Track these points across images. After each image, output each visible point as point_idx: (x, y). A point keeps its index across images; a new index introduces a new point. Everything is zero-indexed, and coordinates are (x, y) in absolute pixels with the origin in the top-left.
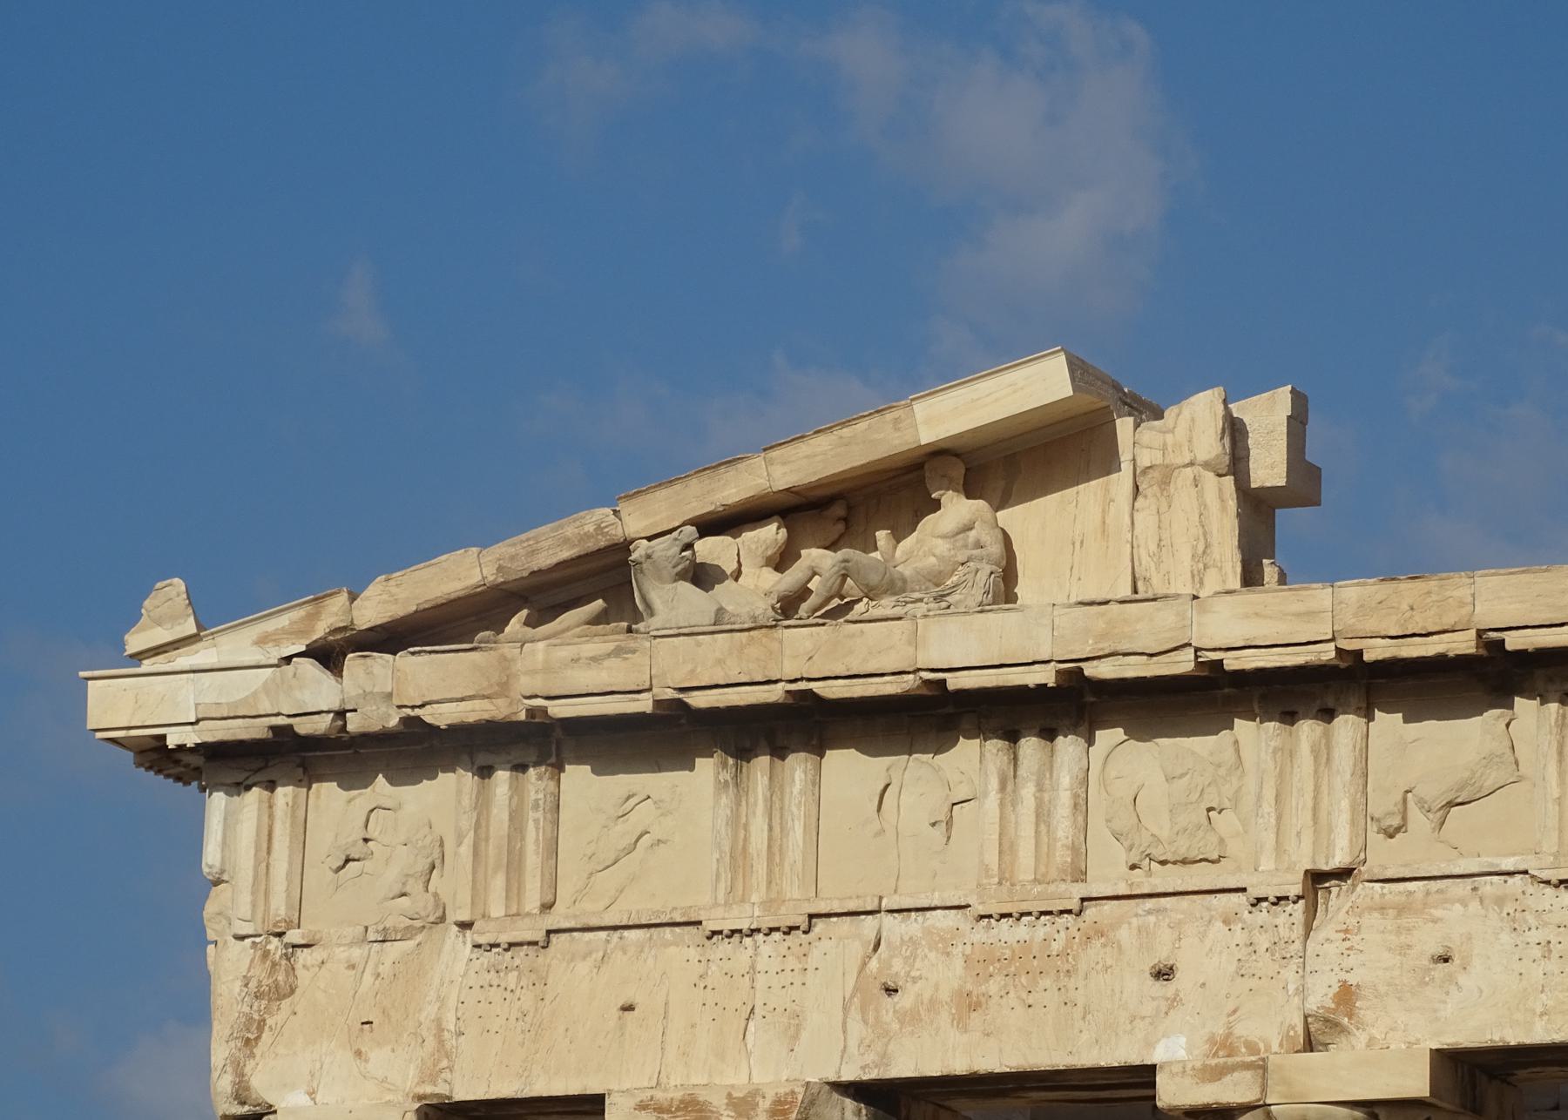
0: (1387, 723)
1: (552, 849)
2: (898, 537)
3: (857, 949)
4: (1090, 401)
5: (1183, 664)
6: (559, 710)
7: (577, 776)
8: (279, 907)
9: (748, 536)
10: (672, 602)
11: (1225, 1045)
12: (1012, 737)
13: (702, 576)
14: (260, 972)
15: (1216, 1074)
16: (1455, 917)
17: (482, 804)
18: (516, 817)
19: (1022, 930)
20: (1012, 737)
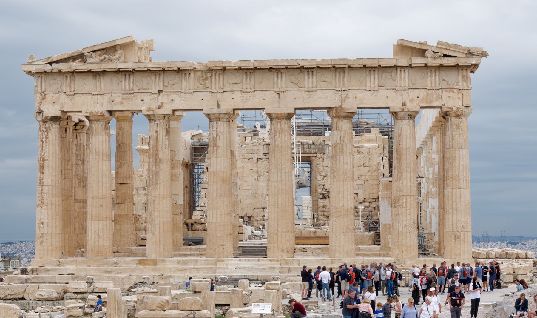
5: (146, 69)
10: (90, 60)
11: (149, 108)
14: (41, 96)
15: (149, 111)
16: (173, 96)
19: (127, 96)
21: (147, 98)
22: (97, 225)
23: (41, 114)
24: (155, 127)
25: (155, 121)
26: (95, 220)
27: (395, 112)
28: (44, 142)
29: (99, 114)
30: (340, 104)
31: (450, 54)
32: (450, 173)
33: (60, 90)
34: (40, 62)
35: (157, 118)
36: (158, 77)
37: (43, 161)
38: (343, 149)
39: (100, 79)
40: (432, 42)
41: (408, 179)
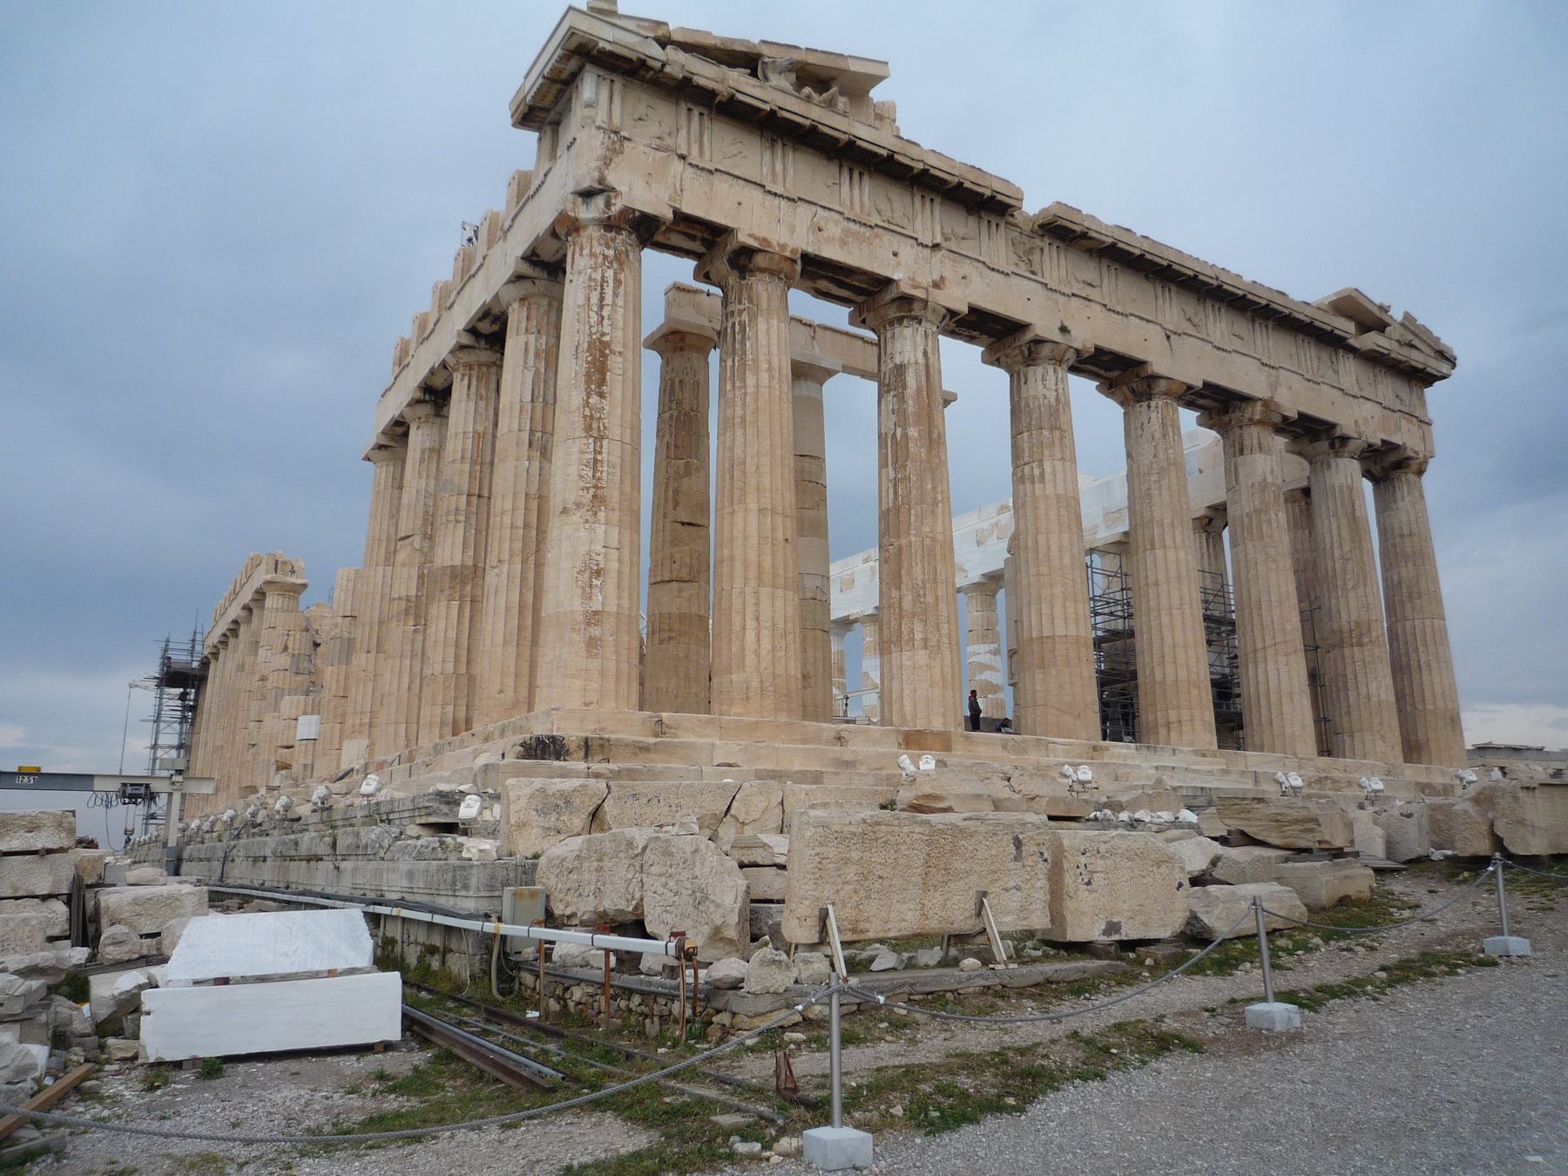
5: (921, 166)
15: (916, 287)
16: (967, 268)
21: (908, 252)
23: (599, 201)
24: (919, 338)
25: (920, 323)
27: (1345, 439)
28: (609, 291)
29: (788, 254)
33: (669, 141)
34: (631, 25)
35: (929, 315)
36: (928, 204)
37: (603, 355)
40: (1397, 314)
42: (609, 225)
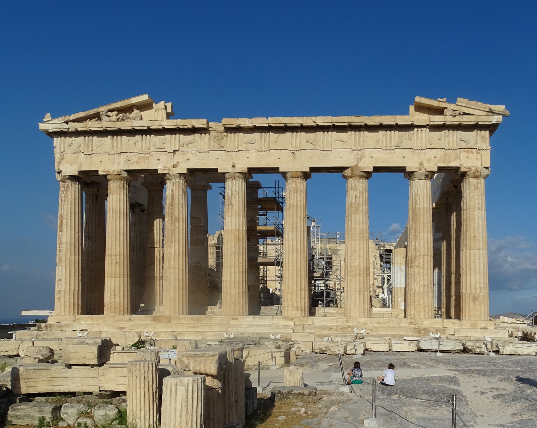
0: (182, 136)
1: (92, 145)
2: (130, 114)
3: (126, 156)
4: (150, 101)
5: (160, 127)
6: (93, 129)
7: (95, 138)
8: (62, 150)
9: (113, 113)
11: (165, 167)
12: (142, 135)
13: (108, 116)
14: (60, 157)
15: (164, 170)
16: (189, 155)
17: (85, 140)
18: (88, 141)
19: (143, 155)
20: (142, 135)
21: (163, 157)
22: (113, 282)
26: (111, 277)
29: (116, 173)
30: (356, 164)
31: (470, 112)
32: (468, 234)
37: (62, 220)
38: (358, 208)
39: (117, 140)
41: (426, 239)
42: (63, 181)
